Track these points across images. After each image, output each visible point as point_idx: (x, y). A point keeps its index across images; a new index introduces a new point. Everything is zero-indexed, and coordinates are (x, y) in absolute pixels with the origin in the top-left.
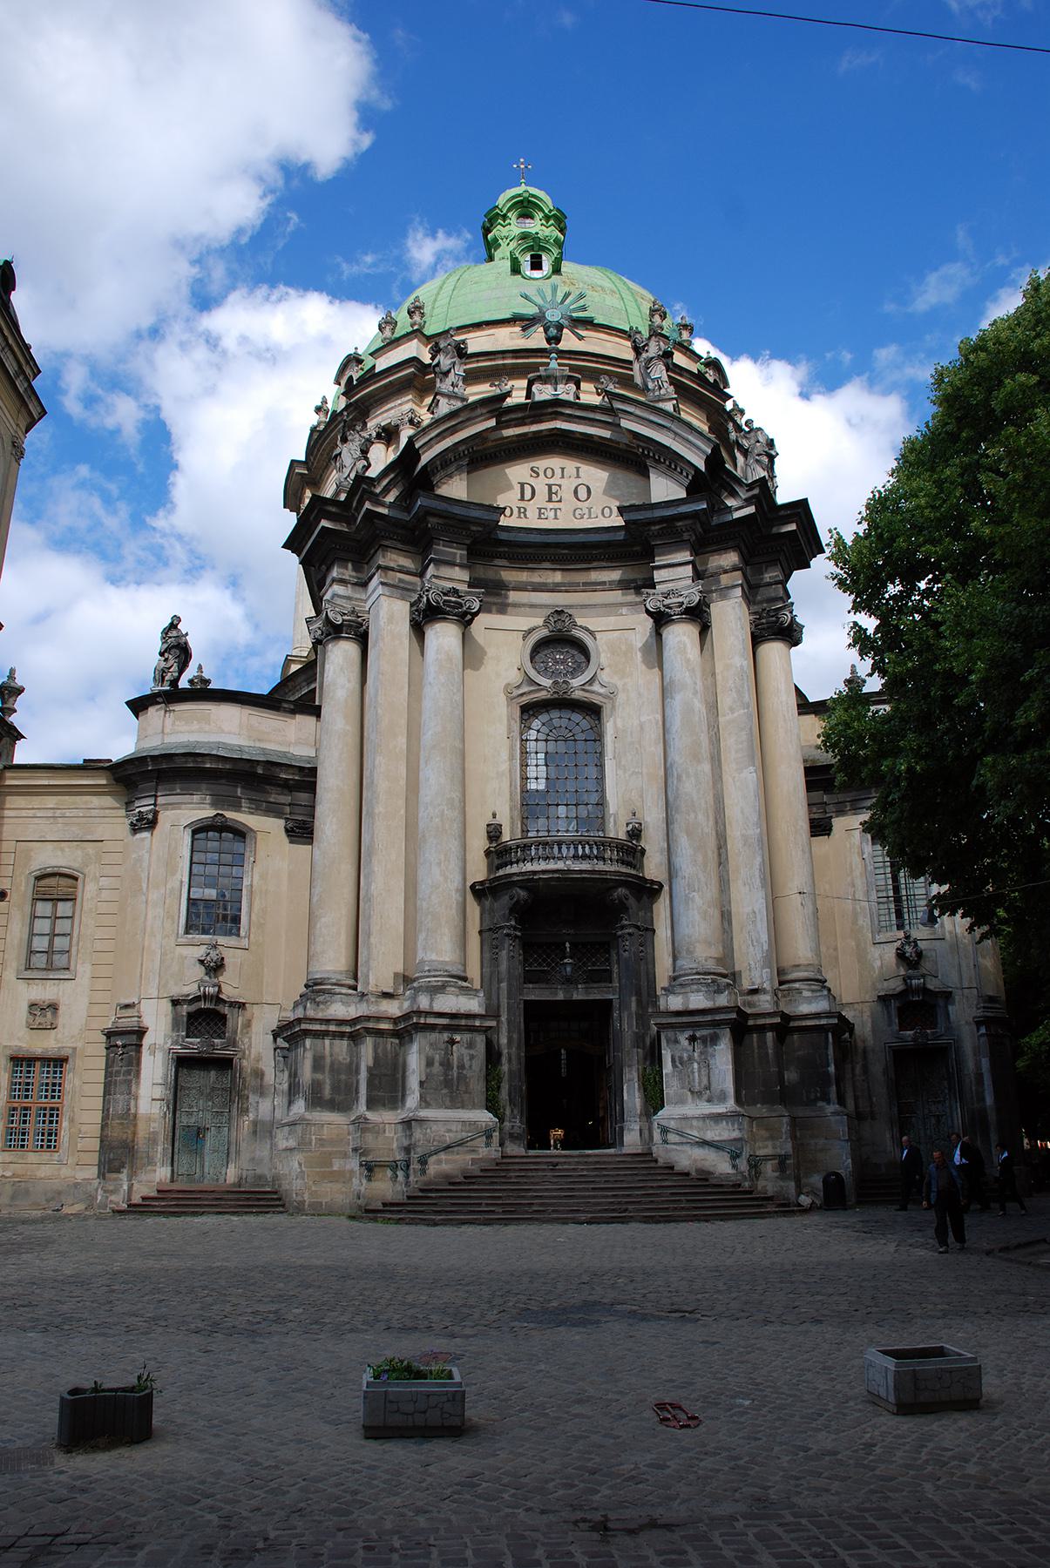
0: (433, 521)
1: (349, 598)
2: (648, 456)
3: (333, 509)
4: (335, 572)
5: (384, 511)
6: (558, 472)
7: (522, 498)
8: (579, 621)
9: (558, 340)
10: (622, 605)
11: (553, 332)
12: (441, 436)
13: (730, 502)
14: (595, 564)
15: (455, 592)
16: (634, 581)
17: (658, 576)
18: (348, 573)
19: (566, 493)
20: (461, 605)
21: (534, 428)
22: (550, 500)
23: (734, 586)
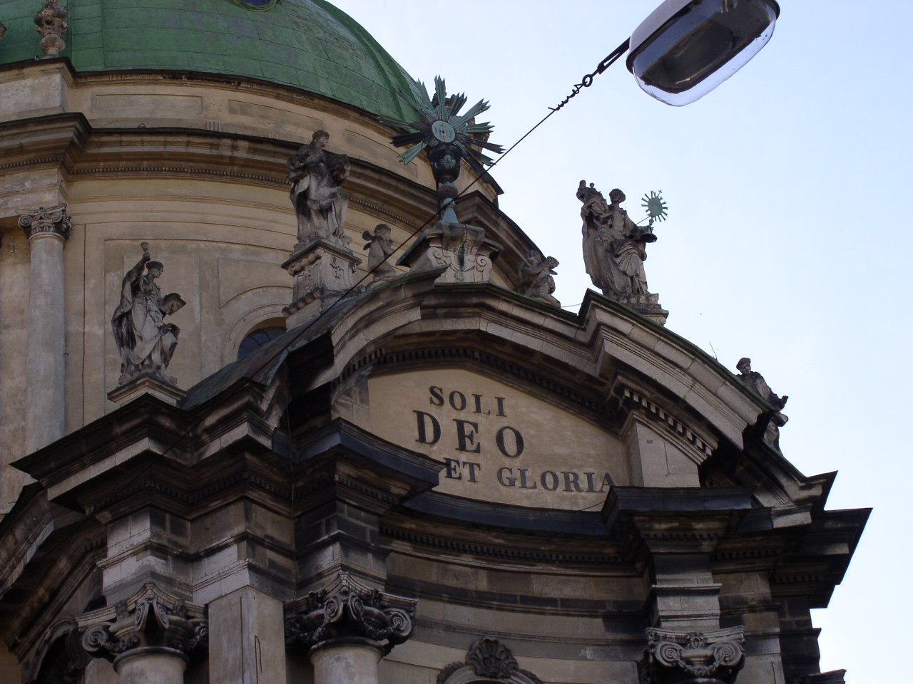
0: (344, 470)
1: (169, 581)
2: (638, 406)
3: (166, 422)
4: (140, 531)
5: (266, 442)
6: (471, 401)
7: (422, 438)
8: (524, 662)
9: (454, 174)
10: (586, 642)
11: (449, 161)
12: (355, 331)
13: (766, 501)
14: (540, 567)
15: (374, 598)
16: (601, 604)
17: (665, 606)
18: (166, 537)
19: (486, 439)
20: (383, 623)
21: (448, 325)
22: (462, 447)
23: (768, 636)
